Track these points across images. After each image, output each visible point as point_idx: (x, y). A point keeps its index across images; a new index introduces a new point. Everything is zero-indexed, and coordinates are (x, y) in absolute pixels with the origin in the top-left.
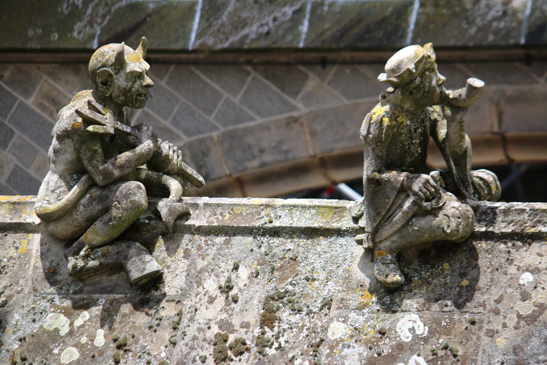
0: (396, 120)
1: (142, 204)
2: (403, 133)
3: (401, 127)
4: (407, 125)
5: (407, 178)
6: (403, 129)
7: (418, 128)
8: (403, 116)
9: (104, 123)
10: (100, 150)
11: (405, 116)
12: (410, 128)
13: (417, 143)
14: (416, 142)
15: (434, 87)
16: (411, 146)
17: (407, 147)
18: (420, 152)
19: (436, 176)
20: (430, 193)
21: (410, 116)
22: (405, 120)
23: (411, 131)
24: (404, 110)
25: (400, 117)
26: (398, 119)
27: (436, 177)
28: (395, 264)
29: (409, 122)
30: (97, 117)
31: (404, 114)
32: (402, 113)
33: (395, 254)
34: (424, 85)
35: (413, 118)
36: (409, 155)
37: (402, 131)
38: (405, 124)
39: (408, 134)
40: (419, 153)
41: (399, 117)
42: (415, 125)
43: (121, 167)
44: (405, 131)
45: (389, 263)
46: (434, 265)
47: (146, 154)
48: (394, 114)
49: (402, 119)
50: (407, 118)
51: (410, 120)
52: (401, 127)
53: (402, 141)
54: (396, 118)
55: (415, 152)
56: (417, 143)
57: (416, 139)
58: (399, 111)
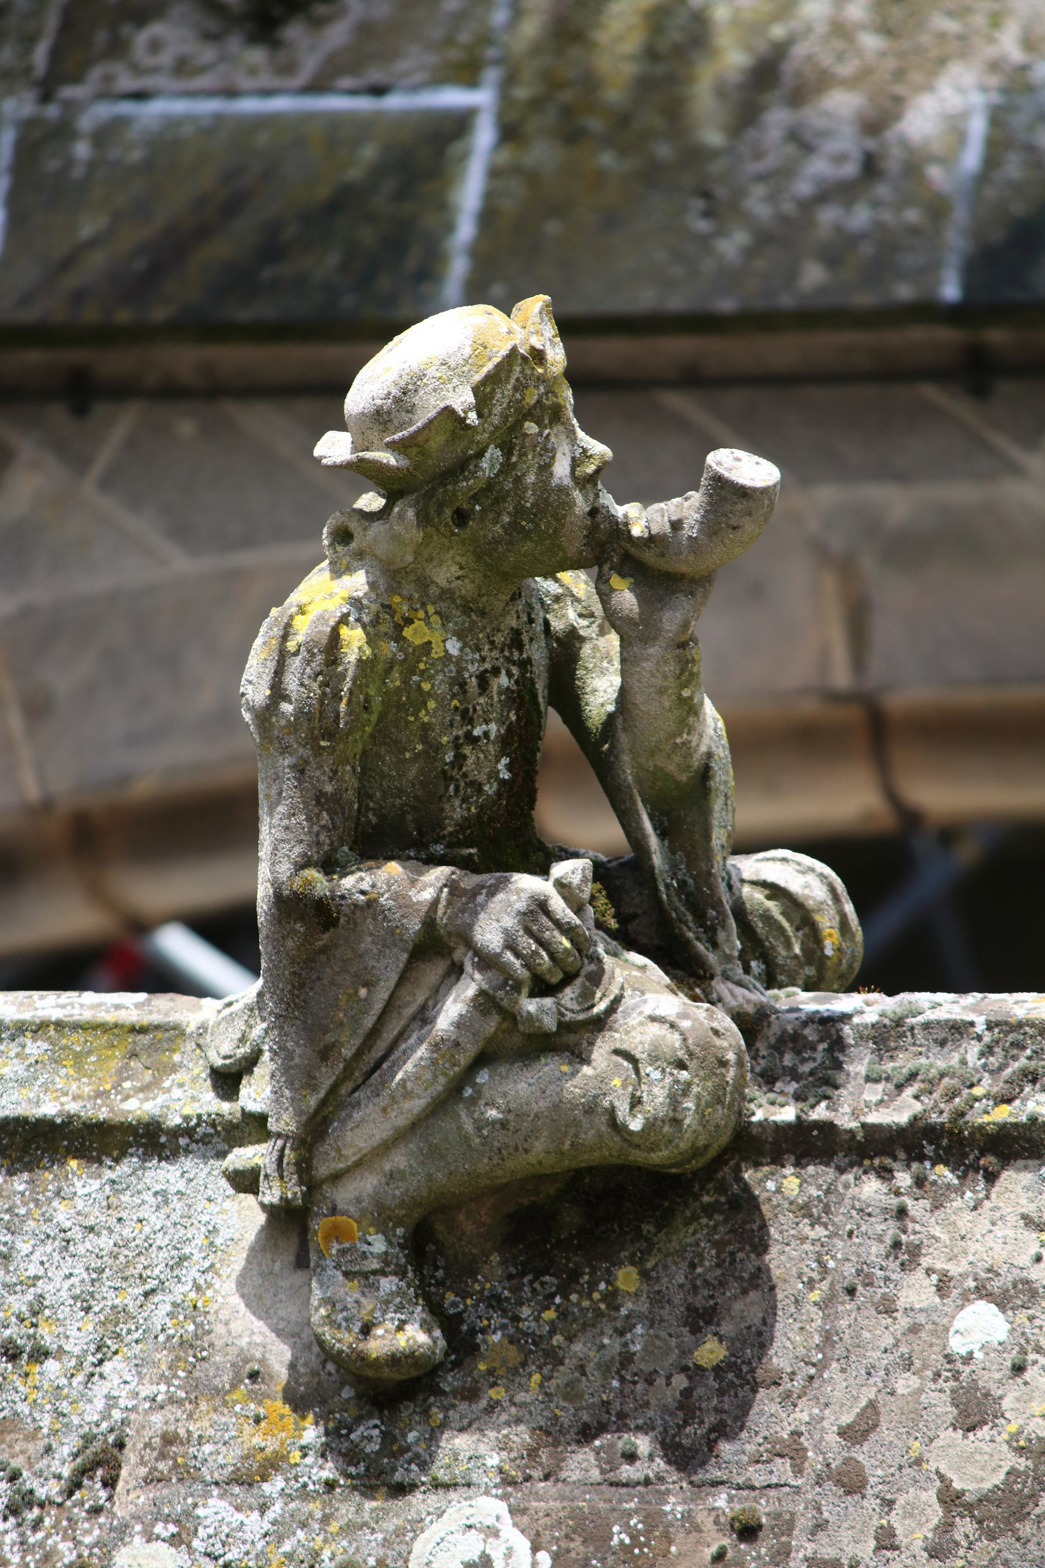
0: (399, 638)
3: (422, 666)
4: (448, 656)
6: (431, 678)
7: (496, 671)
8: (427, 619)
11: (435, 619)
12: (460, 670)
14: (486, 734)
15: (562, 490)
16: (467, 750)
17: (449, 757)
18: (505, 775)
20: (552, 955)
21: (459, 618)
22: (436, 638)
23: (463, 684)
24: (433, 590)
25: (417, 623)
26: (407, 632)
28: (402, 1274)
29: (453, 647)
31: (431, 609)
32: (423, 605)
33: (400, 1231)
34: (518, 480)
36: (457, 789)
37: (426, 686)
38: (437, 653)
39: (454, 696)
40: (503, 782)
41: (409, 621)
42: (483, 659)
44: (439, 684)
45: (374, 1272)
46: (574, 1276)
48: (387, 607)
51: (460, 635)
52: (422, 666)
53: (426, 728)
54: (399, 628)
55: (482, 777)
57: (487, 722)
58: (410, 598)
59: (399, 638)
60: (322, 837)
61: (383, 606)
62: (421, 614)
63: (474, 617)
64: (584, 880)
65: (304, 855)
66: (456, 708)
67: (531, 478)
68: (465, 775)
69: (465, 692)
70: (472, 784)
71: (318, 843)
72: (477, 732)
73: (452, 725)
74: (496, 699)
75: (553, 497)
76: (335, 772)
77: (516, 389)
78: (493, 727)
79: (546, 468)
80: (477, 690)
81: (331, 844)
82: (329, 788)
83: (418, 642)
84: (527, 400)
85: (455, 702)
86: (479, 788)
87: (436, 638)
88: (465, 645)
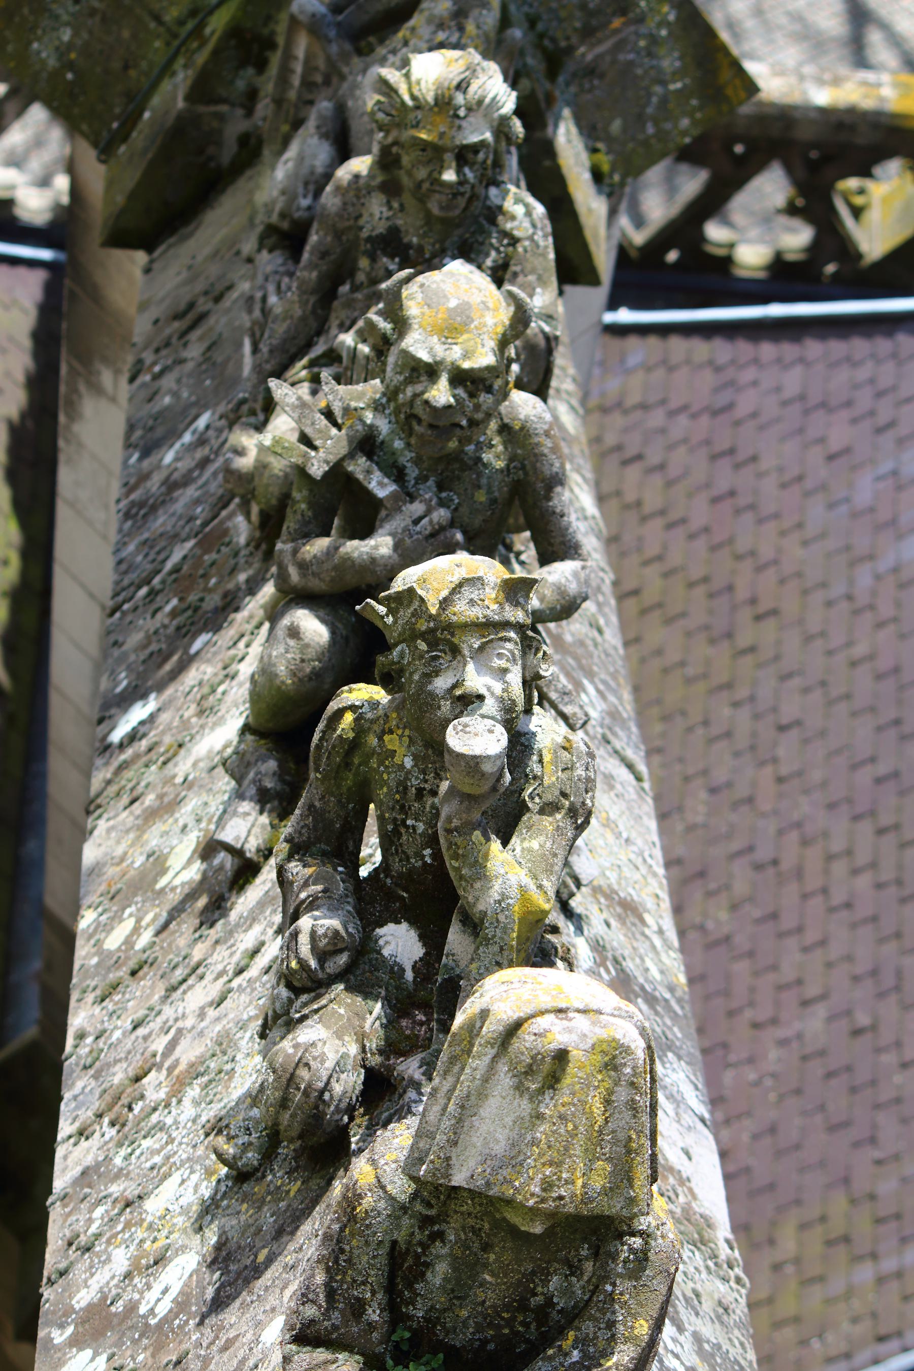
0: (381, 739)
1: (276, 675)
2: (386, 783)
4: (402, 766)
5: (311, 902)
6: (389, 773)
8: (401, 737)
9: (318, 443)
10: (303, 506)
12: (407, 779)
13: (420, 831)
14: (414, 827)
15: (432, 695)
19: (321, 931)
21: (418, 748)
22: (401, 751)
23: (406, 788)
26: (386, 738)
27: (320, 937)
29: (408, 763)
30: (309, 422)
31: (407, 732)
32: (405, 728)
34: (411, 674)
35: (425, 758)
36: (397, 850)
37: (385, 776)
38: (397, 760)
39: (398, 792)
40: (425, 863)
41: (391, 732)
42: (426, 781)
43: (303, 566)
44: (390, 778)
47: (360, 566)
49: (397, 743)
50: (409, 746)
51: (415, 757)
54: (383, 733)
55: (410, 852)
56: (420, 831)
57: (417, 820)
59: (381, 739)
60: (303, 831)
61: (386, 715)
62: (400, 732)
63: (430, 752)
64: (325, 935)
65: (290, 834)
66: (398, 801)
67: (416, 677)
68: (401, 845)
69: (405, 794)
70: (404, 852)
71: (300, 833)
72: (409, 822)
73: (393, 808)
74: (428, 809)
75: (423, 696)
76: (323, 797)
77: (413, 615)
78: (421, 827)
79: (429, 677)
80: (413, 797)
81: (309, 838)
82: (317, 804)
83: (389, 747)
84: (418, 626)
85: (398, 797)
86: (408, 858)
87: (401, 751)
88: (415, 765)
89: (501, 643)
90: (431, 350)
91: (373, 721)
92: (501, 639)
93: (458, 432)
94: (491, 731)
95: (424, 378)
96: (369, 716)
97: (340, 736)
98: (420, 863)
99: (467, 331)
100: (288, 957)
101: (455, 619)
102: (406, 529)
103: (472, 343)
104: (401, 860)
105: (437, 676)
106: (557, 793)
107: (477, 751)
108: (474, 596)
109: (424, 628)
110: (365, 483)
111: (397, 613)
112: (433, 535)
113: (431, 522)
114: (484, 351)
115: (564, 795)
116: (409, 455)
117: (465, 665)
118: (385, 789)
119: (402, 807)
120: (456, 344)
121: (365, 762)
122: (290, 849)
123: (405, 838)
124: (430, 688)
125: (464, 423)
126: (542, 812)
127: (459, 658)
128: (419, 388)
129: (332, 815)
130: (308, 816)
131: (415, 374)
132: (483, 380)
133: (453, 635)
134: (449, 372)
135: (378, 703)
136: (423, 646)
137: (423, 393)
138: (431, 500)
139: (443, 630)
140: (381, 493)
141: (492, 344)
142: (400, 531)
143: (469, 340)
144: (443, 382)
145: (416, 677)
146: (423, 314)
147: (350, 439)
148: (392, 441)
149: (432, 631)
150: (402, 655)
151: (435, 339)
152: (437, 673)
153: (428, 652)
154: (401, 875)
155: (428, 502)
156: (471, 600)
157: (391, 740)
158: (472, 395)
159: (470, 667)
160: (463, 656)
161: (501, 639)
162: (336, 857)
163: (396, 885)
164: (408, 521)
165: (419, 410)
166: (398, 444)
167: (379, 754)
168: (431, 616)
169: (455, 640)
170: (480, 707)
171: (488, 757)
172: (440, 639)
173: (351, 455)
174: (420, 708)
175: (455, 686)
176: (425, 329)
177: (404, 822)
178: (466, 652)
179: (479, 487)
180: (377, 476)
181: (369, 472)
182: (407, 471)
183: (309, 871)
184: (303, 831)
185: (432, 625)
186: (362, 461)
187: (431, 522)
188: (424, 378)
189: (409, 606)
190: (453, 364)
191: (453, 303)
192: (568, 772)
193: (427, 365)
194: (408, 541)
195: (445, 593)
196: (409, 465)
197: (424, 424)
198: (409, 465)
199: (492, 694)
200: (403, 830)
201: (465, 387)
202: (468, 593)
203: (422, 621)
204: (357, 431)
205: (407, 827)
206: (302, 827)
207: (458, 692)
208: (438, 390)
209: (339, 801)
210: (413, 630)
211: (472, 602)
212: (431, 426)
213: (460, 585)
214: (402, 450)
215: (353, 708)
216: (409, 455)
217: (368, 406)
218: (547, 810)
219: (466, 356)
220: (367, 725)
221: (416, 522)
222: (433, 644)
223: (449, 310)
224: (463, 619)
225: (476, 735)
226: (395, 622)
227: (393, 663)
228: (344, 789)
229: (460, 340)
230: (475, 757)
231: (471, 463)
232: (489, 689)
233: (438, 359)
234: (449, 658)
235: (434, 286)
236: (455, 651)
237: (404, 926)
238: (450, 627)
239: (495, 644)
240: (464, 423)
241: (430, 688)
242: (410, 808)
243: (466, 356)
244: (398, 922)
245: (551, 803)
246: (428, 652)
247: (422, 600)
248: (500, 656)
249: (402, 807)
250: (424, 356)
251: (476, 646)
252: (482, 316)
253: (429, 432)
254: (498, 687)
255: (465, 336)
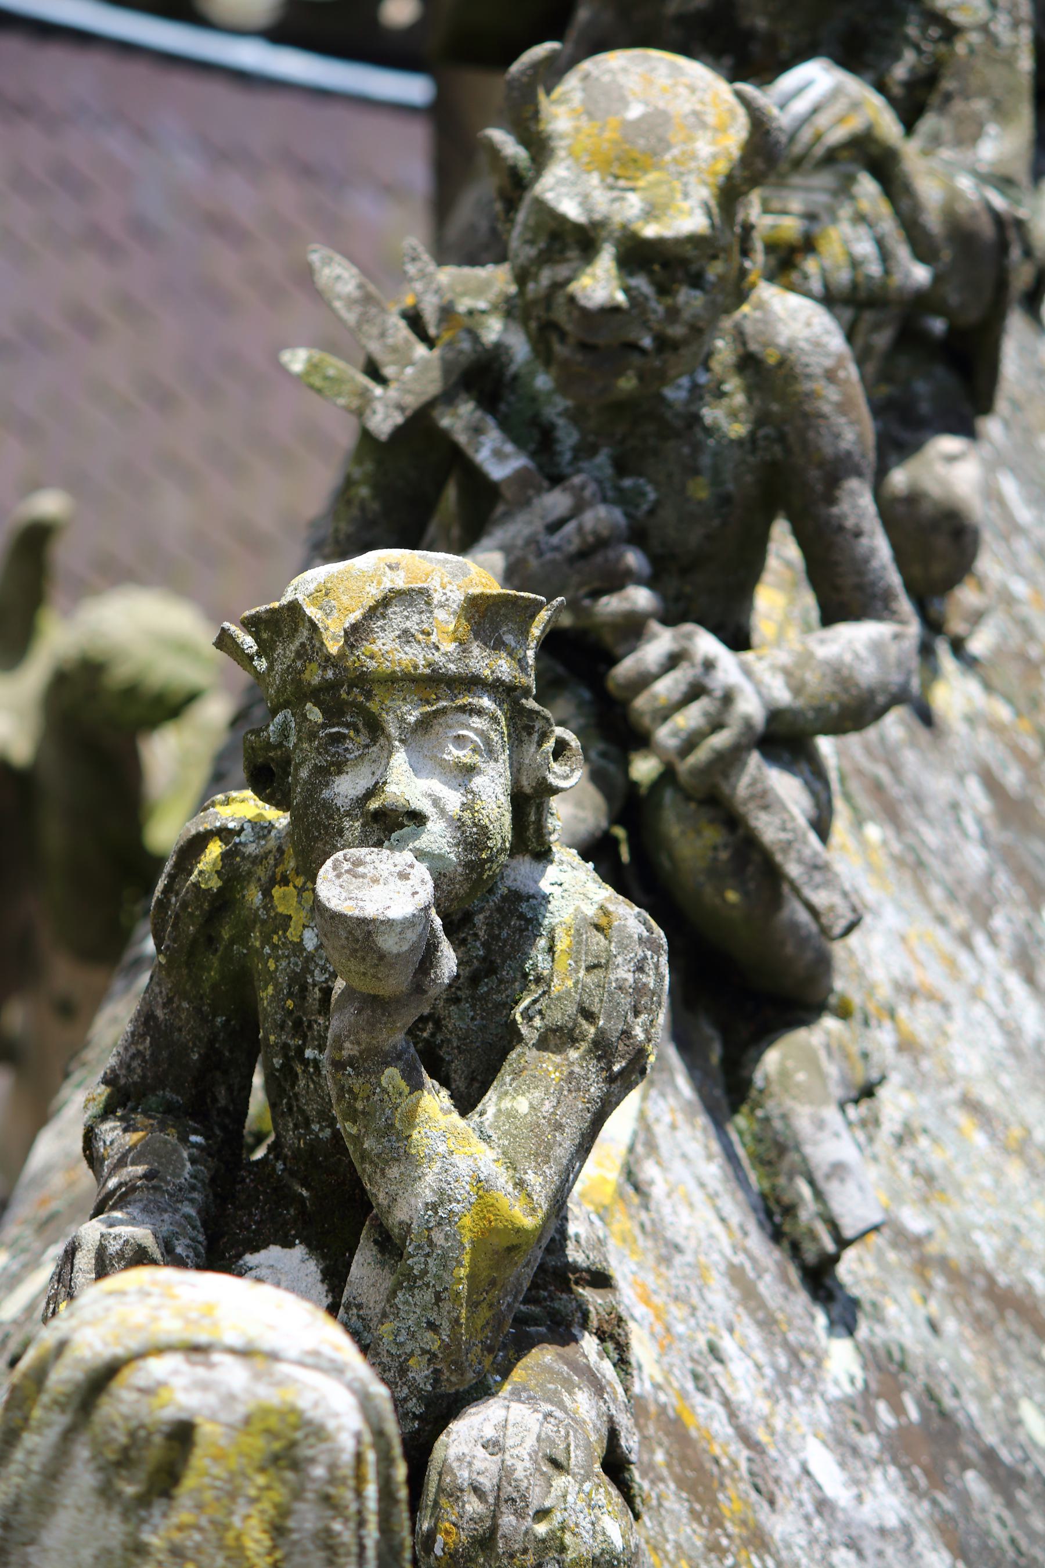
0: (267, 893)
2: (272, 977)
4: (299, 946)
6: (277, 960)
12: (306, 970)
15: (329, 808)
19: (113, 1247)
23: (304, 988)
26: (277, 892)
36: (290, 1109)
38: (292, 934)
39: (290, 995)
41: (285, 881)
49: (294, 901)
54: (272, 882)
55: (312, 1109)
59: (267, 893)
61: (280, 850)
65: (113, 1070)
66: (291, 1012)
67: (304, 773)
68: (296, 1095)
69: (304, 998)
70: (302, 1111)
71: (129, 1066)
72: (309, 1053)
75: (313, 809)
76: (170, 1001)
77: (299, 655)
80: (316, 1006)
81: (144, 1077)
82: (160, 1013)
83: (280, 910)
84: (306, 676)
86: (307, 1122)
89: (464, 717)
90: (585, 201)
91: (257, 860)
92: (462, 709)
93: (636, 359)
94: (403, 876)
95: (573, 253)
96: (251, 849)
97: (196, 885)
98: (328, 1132)
99: (657, 167)
100: (56, 1294)
101: (372, 665)
102: (532, 541)
103: (664, 190)
104: (296, 1127)
105: (340, 772)
106: (572, 1009)
107: (370, 911)
108: (412, 625)
109: (316, 680)
110: (470, 451)
111: (273, 649)
112: (584, 554)
113: (580, 529)
114: (686, 205)
115: (589, 1016)
116: (562, 403)
117: (390, 754)
118: (270, 989)
119: (298, 1024)
120: (633, 189)
121: (241, 938)
122: (110, 1097)
123: (302, 1083)
124: (326, 794)
125: (647, 342)
126: (542, 1044)
127: (382, 741)
128: (562, 271)
129: (185, 1036)
130: (143, 1036)
131: (557, 246)
132: (684, 262)
133: (369, 695)
134: (618, 244)
135: (271, 826)
136: (315, 715)
137: (569, 281)
138: (583, 487)
139: (351, 686)
140: (497, 472)
141: (704, 193)
142: (520, 542)
143: (658, 184)
144: (605, 262)
145: (304, 773)
146: (577, 130)
147: (447, 368)
148: (532, 375)
149: (331, 687)
150: (284, 731)
151: (595, 179)
152: (339, 767)
153: (324, 726)
154: (297, 1153)
155: (578, 493)
156: (405, 631)
157: (284, 897)
158: (663, 290)
159: (400, 759)
160: (388, 737)
161: (462, 709)
162: (193, 1116)
163: (292, 1174)
164: (538, 525)
165: (561, 315)
166: (543, 382)
167: (264, 922)
168: (328, 658)
169: (373, 706)
170: (416, 836)
171: (390, 923)
172: (346, 702)
173: (447, 398)
174: (307, 832)
175: (371, 793)
176: (577, 159)
177: (300, 1051)
178: (393, 730)
179: (695, 471)
180: (493, 438)
181: (477, 430)
182: (560, 434)
183: (132, 1138)
184: (135, 1064)
185: (330, 674)
186: (467, 409)
187: (580, 529)
188: (573, 253)
189: (292, 636)
190: (624, 227)
191: (635, 112)
192: (599, 973)
193: (578, 227)
194: (534, 563)
195: (356, 616)
196: (561, 422)
197: (571, 340)
198: (561, 422)
199: (442, 812)
200: (299, 1069)
201: (650, 273)
202: (398, 617)
203: (314, 666)
204: (461, 352)
205: (305, 1062)
206: (133, 1057)
207: (374, 805)
208: (594, 276)
209: (198, 1010)
210: (298, 683)
211: (406, 636)
212: (584, 346)
213: (384, 602)
214: (550, 394)
215: (223, 833)
216: (562, 403)
217: (494, 308)
218: (553, 1040)
219: (651, 213)
220: (246, 867)
221: (554, 527)
222: (333, 712)
223: (626, 124)
224: (386, 667)
225: (375, 881)
226: (270, 668)
227: (268, 746)
228: (206, 987)
229: (641, 183)
230: (363, 921)
231: (679, 424)
232: (436, 802)
233: (597, 217)
234: (363, 739)
235: (606, 78)
236: (375, 728)
237: (299, 1251)
238: (363, 681)
239: (452, 718)
240: (647, 342)
241: (326, 794)
242: (310, 1027)
243: (651, 213)
244: (287, 1244)
245: (560, 1029)
246: (324, 726)
247: (314, 627)
248: (460, 741)
249: (298, 1024)
250: (571, 209)
251: (411, 719)
252: (690, 139)
253: (579, 357)
254: (453, 800)
255: (653, 176)
